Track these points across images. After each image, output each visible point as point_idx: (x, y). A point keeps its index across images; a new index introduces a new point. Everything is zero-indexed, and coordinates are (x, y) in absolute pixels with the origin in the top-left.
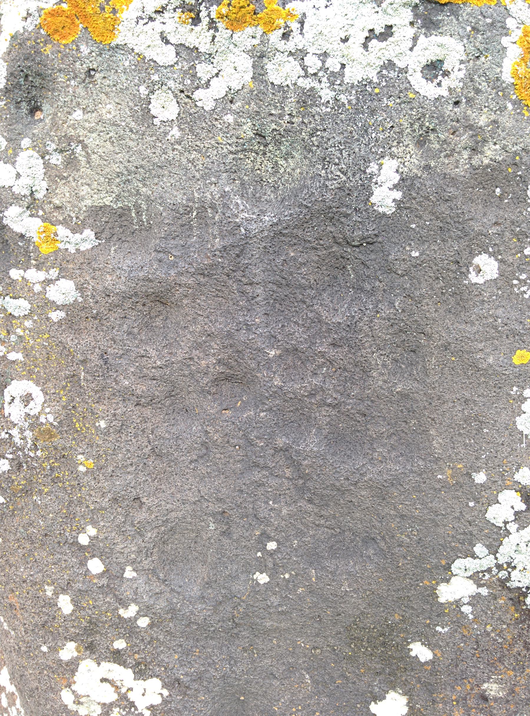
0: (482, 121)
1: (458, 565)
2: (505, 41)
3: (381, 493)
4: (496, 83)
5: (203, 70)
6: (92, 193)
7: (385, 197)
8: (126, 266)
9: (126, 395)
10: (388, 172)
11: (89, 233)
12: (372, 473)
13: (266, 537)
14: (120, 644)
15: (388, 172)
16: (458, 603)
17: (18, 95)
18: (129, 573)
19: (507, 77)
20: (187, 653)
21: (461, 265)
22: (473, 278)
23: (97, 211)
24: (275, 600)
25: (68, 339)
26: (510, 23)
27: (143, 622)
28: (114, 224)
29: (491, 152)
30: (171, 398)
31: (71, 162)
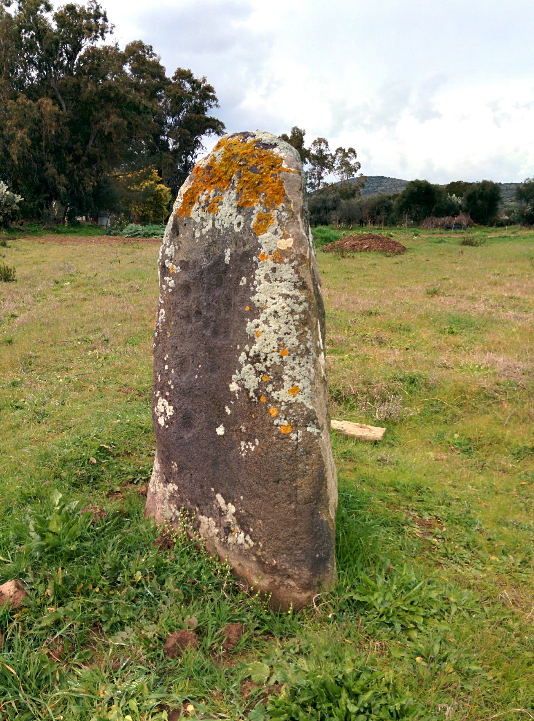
0: (245, 239)
1: (234, 377)
2: (252, 216)
3: (220, 349)
4: (250, 229)
5: (204, 223)
6: (182, 257)
7: (227, 259)
8: (185, 277)
9: (178, 314)
10: (228, 252)
11: (179, 267)
12: (219, 344)
13: (199, 364)
14: (167, 394)
15: (228, 252)
16: (234, 392)
17: (174, 230)
18: (173, 371)
19: (251, 227)
20: (180, 400)
21: (239, 279)
22: (241, 284)
23: (182, 262)
24: (197, 384)
25: (171, 297)
26: (254, 212)
27: (172, 387)
28: (184, 265)
29: (247, 247)
30: (187, 318)
31: (179, 248)
